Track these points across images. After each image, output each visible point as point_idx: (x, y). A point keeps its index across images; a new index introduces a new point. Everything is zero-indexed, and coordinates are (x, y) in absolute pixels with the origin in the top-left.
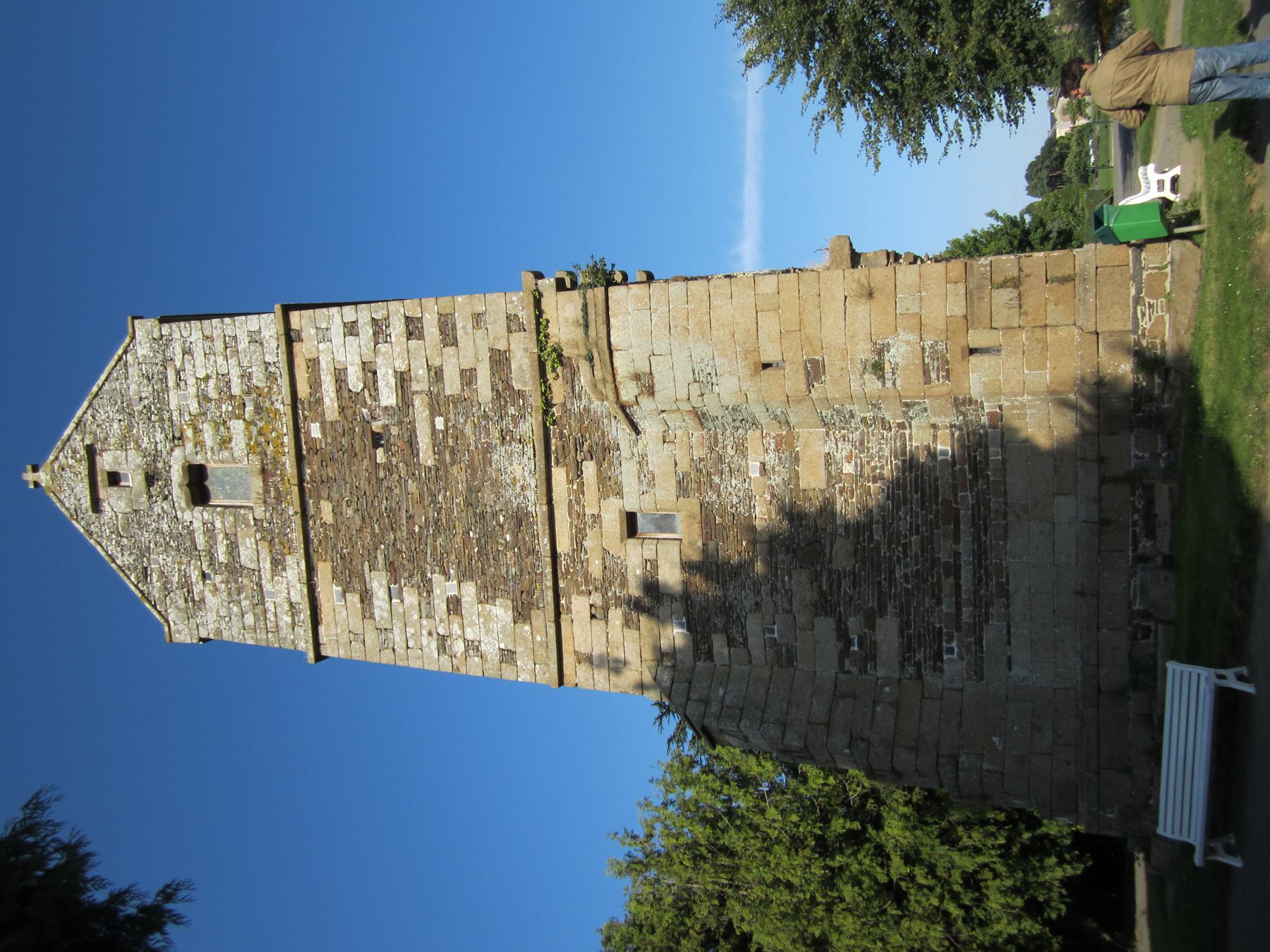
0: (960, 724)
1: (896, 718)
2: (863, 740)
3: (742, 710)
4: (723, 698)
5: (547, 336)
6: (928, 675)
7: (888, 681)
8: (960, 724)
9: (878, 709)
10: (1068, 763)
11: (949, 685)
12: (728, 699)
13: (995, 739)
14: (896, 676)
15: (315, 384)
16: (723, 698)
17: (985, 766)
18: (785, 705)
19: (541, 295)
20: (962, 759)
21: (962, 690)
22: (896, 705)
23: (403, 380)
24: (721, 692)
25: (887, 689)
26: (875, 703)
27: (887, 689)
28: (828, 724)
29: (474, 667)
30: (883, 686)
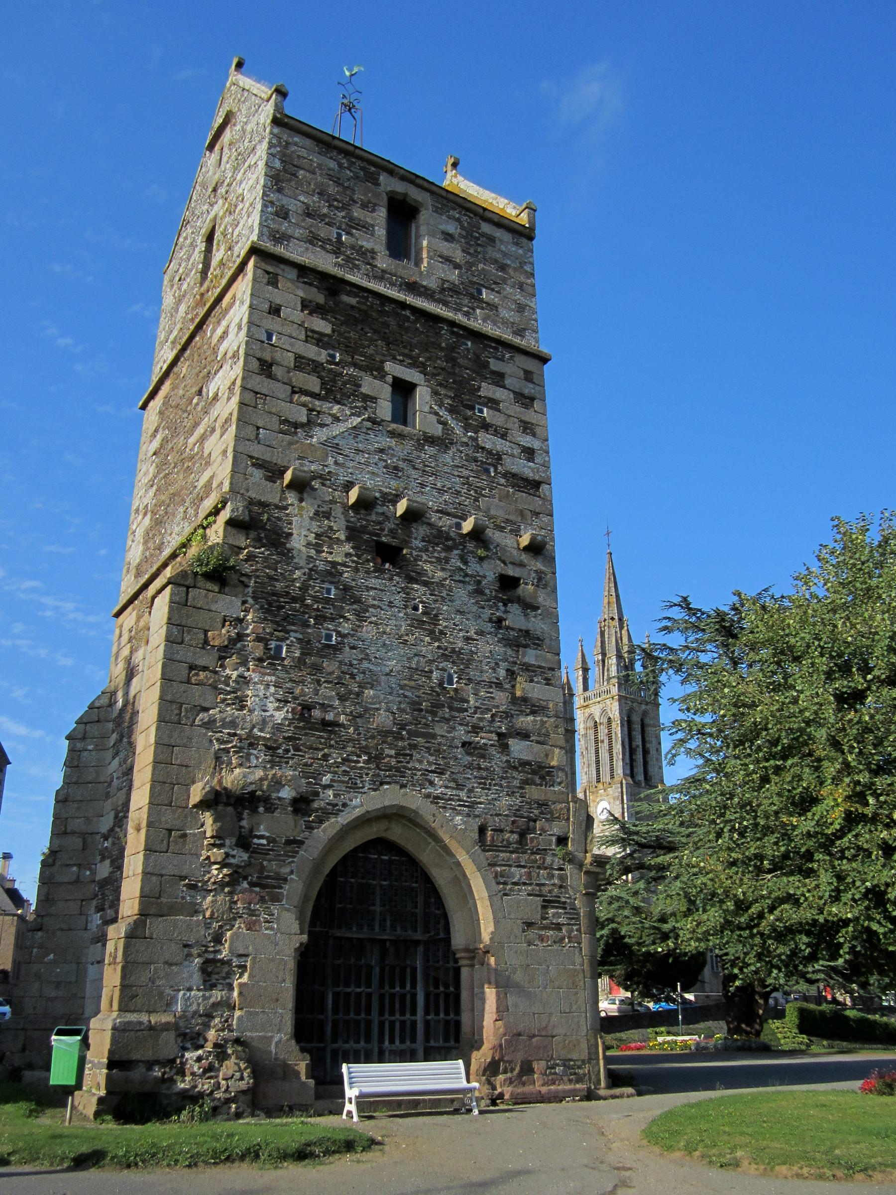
0: (62, 930)
1: (69, 883)
2: (54, 861)
3: (77, 766)
4: (86, 750)
5: (209, 525)
6: (94, 903)
7: (93, 873)
8: (62, 930)
9: (75, 869)
10: (34, 1008)
11: (90, 919)
12: (85, 753)
13: (52, 955)
14: (97, 879)
15: (227, 310)
16: (86, 750)
17: (35, 950)
18: (79, 798)
19: (224, 507)
20: (40, 934)
21: (86, 929)
22: (77, 881)
23: (216, 398)
24: (91, 747)
25: (88, 873)
26: (79, 866)
27: (88, 873)
28: (65, 833)
29: (129, 542)
30: (90, 869)
